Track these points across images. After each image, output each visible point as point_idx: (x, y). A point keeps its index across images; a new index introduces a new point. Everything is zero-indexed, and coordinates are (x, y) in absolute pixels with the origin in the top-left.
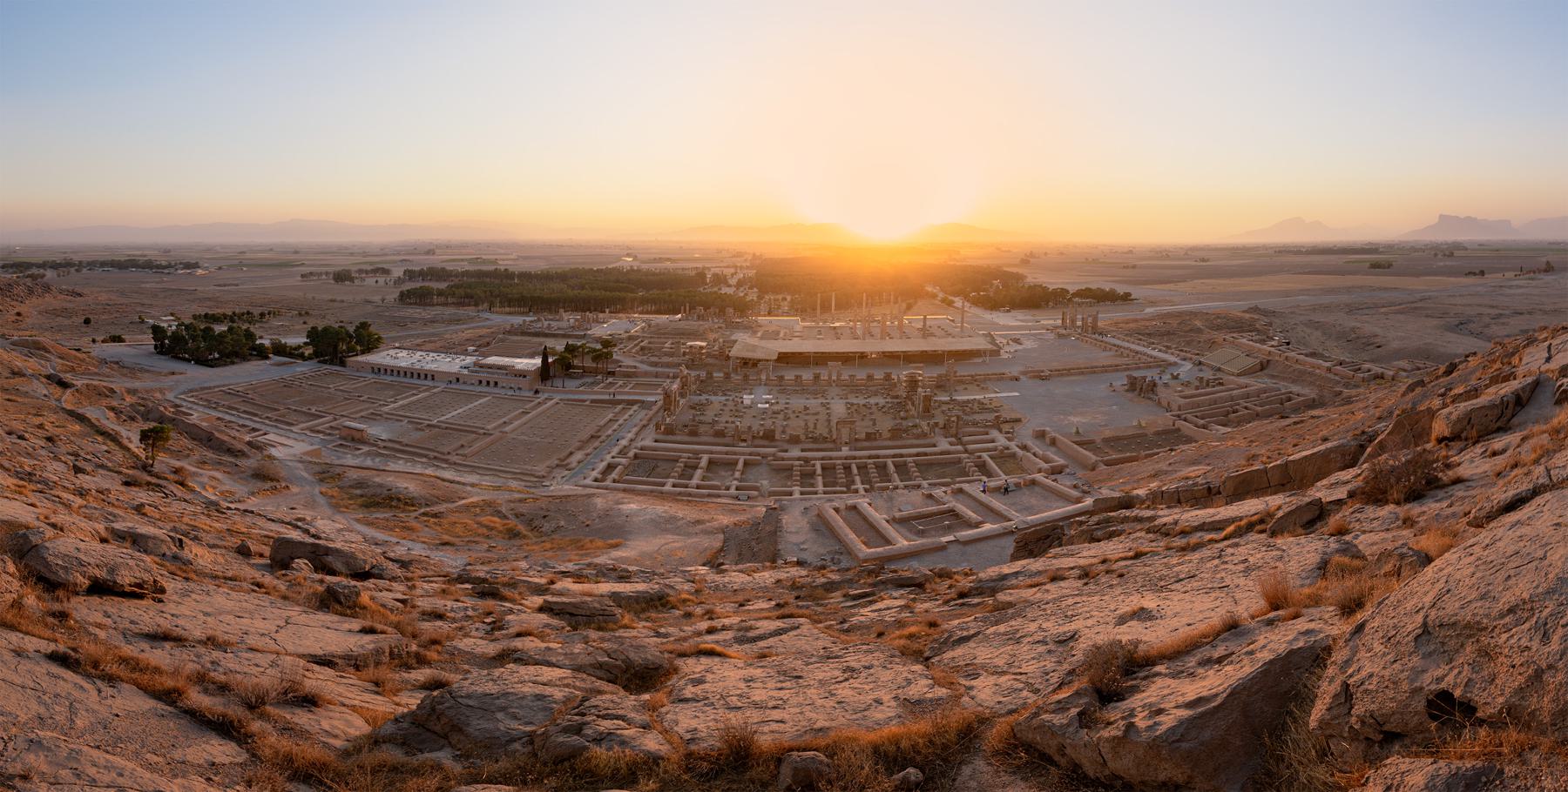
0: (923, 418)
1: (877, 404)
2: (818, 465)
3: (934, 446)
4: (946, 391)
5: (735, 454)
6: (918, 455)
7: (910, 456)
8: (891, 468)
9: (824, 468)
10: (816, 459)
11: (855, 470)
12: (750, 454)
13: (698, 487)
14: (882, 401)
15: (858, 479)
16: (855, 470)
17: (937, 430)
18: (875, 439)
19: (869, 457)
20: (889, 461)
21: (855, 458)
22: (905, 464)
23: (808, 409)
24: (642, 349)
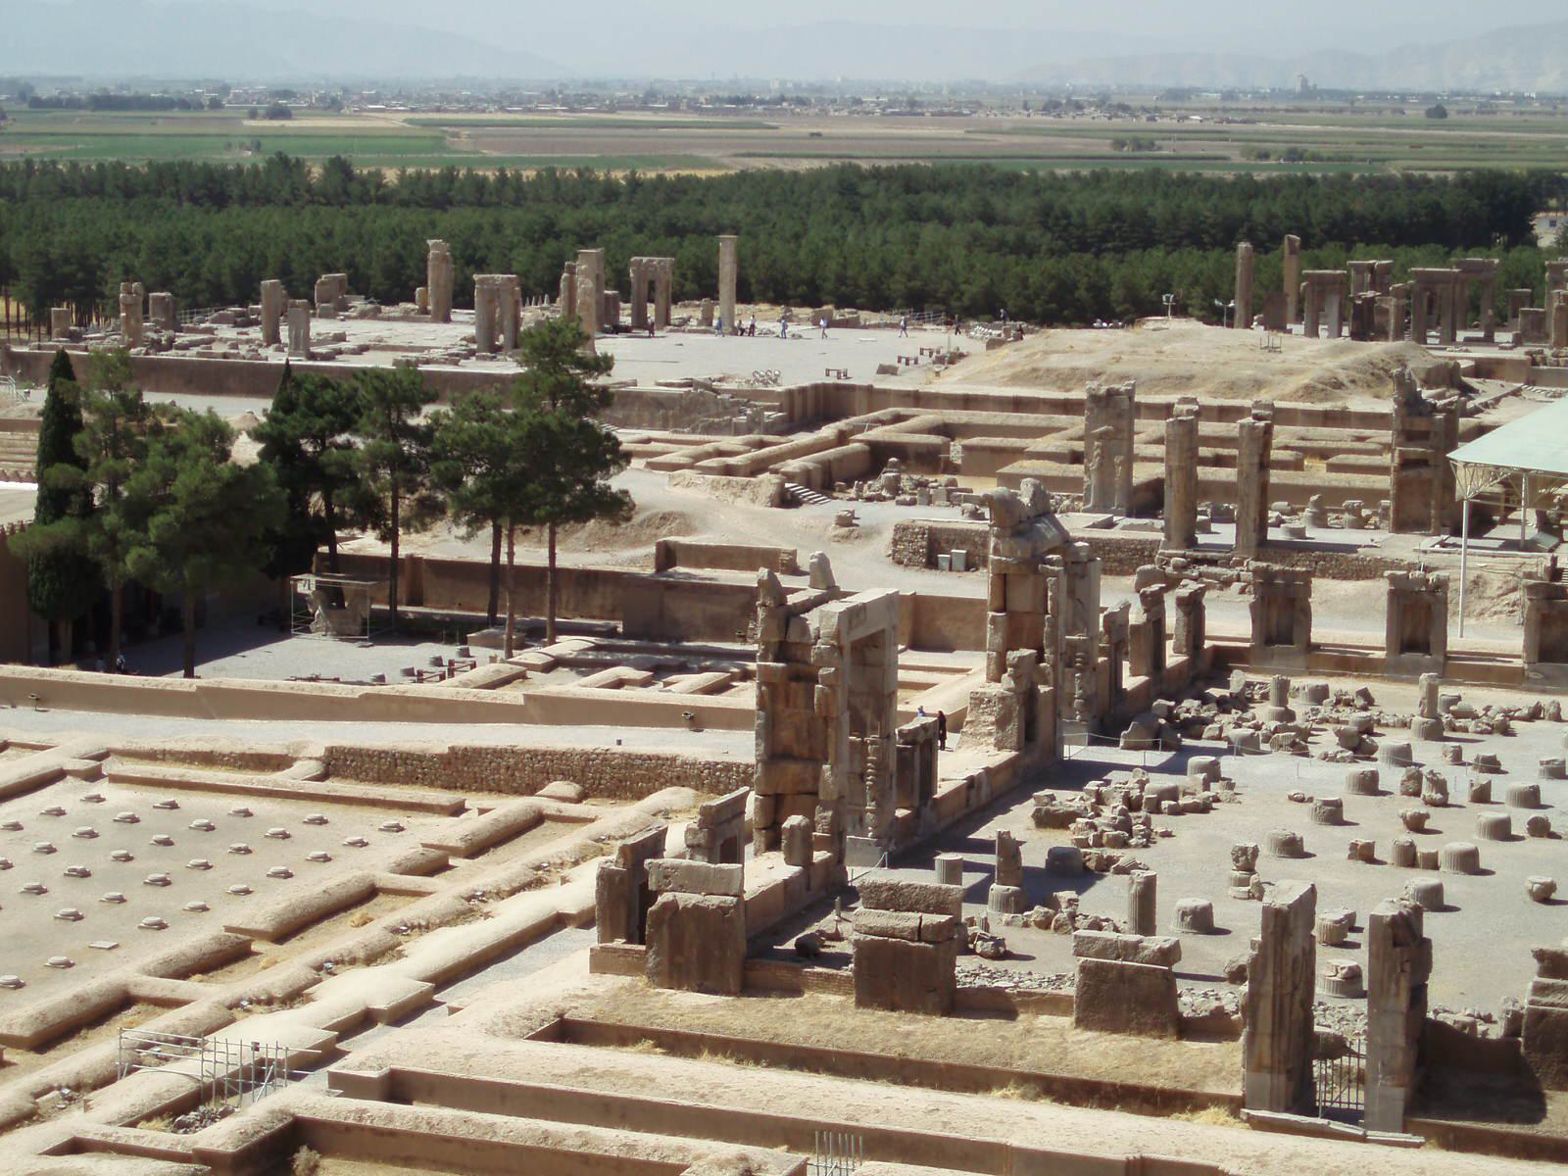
24: (878, 456)
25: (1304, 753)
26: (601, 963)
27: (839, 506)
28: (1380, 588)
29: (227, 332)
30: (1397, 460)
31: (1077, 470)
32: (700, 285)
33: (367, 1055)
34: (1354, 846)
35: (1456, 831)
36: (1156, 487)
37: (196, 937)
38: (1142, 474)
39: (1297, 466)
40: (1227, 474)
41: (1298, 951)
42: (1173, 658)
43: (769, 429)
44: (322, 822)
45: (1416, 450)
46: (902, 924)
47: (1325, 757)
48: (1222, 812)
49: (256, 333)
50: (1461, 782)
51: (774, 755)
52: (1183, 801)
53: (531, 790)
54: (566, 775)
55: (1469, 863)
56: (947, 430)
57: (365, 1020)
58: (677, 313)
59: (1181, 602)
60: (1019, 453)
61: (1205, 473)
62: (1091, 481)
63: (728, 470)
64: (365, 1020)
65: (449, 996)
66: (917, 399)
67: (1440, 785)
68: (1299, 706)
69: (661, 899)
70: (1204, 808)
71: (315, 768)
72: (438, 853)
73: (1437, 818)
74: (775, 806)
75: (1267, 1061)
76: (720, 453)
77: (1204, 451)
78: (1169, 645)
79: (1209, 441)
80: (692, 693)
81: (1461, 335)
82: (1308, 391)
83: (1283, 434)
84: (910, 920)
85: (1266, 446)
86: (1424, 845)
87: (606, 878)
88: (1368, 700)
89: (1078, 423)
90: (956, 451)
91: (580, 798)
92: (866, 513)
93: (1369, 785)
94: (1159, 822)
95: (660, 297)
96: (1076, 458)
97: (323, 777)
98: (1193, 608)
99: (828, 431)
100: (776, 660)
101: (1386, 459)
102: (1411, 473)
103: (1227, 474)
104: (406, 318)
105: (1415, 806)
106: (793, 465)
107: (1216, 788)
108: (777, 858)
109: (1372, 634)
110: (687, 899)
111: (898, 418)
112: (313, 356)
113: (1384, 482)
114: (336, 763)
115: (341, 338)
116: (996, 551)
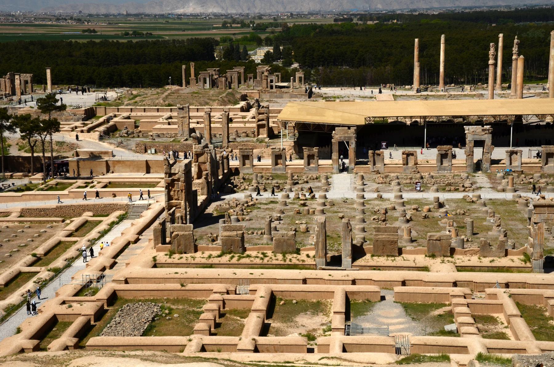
23: (441, 205)
30: (257, 120)
45: (261, 117)
46: (233, 234)
52: (250, 204)
54: (88, 211)
62: (181, 128)
72: (71, 232)
75: (321, 256)
80: (77, 188)
84: (235, 233)
100: (169, 177)
102: (260, 123)
109: (267, 162)
110: (181, 233)
113: (254, 125)
116: (195, 148)
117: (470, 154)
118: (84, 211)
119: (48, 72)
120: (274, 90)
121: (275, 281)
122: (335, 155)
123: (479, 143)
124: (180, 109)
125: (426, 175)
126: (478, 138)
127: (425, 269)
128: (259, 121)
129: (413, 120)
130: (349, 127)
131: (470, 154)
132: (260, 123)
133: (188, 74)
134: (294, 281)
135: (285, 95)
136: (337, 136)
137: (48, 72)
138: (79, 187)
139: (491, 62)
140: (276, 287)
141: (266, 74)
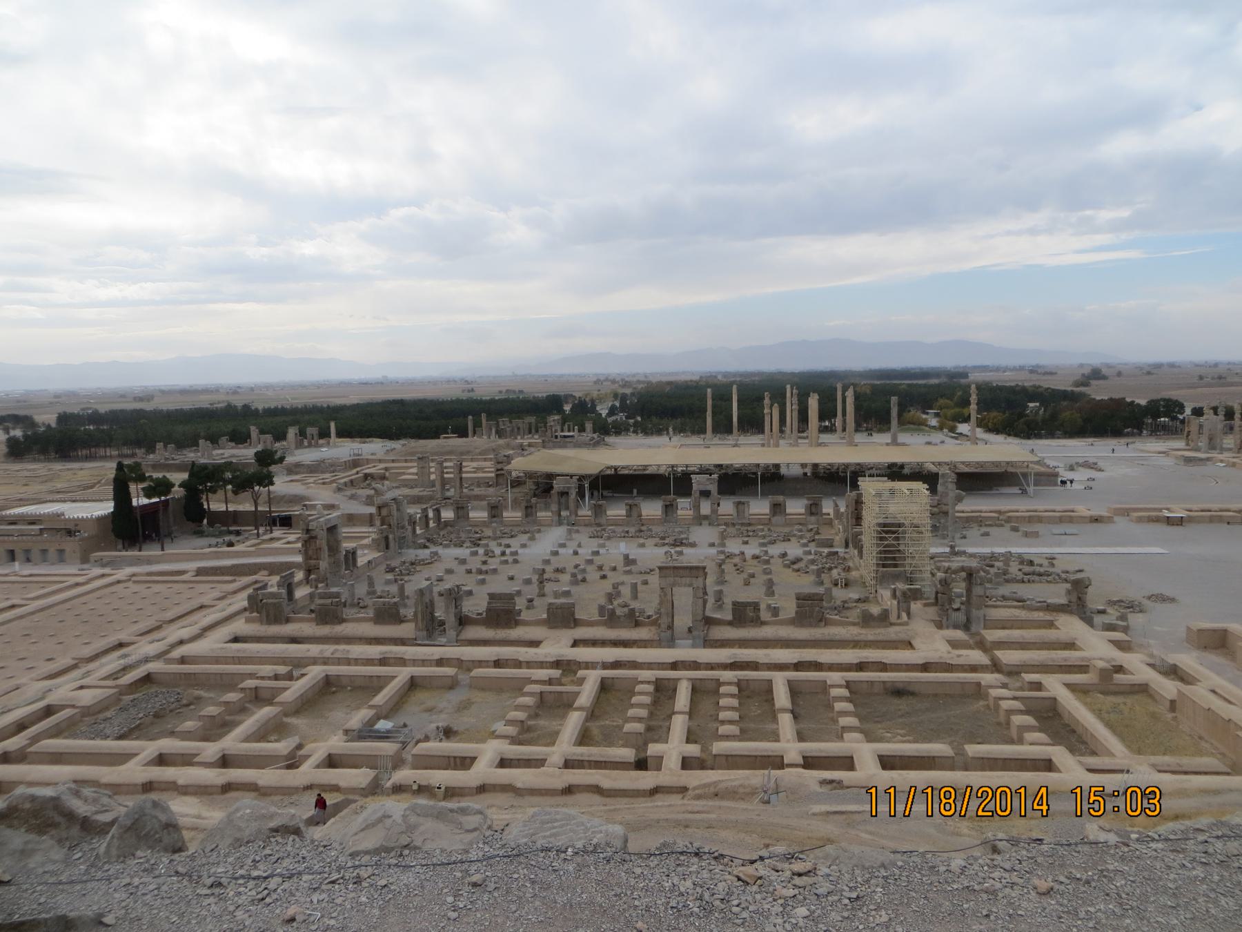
0: (882, 580)
1: (784, 555)
2: (592, 678)
3: (909, 645)
4: (944, 537)
5: (402, 662)
6: (860, 667)
7: (832, 667)
8: (782, 697)
9: (605, 687)
10: (589, 665)
11: (683, 698)
12: (440, 662)
13: (225, 761)
14: (794, 550)
15: (679, 724)
16: (683, 698)
17: (916, 606)
18: (758, 622)
19: (734, 666)
20: (780, 681)
21: (695, 666)
22: (824, 687)
23: (634, 562)
24: (366, 476)
25: (462, 546)
26: (248, 621)
27: (354, 491)
28: (485, 503)
29: (192, 455)
31: (416, 477)
32: (324, 434)
33: (177, 653)
34: (466, 570)
35: (493, 563)
36: (434, 481)
37: (143, 625)
38: (433, 477)
39: (475, 472)
40: (452, 476)
41: (427, 600)
42: (432, 524)
43: (339, 471)
44: (149, 588)
45: (499, 466)
47: (467, 547)
48: (436, 564)
49: (199, 454)
50: (498, 551)
51: (307, 557)
53: (255, 573)
54: (264, 569)
55: (495, 571)
56: (386, 469)
57: (181, 642)
58: (321, 442)
59: (434, 510)
60: (404, 474)
61: (446, 476)
63: (324, 483)
64: (181, 642)
65: (207, 633)
66: (380, 461)
67: (493, 552)
68: (463, 535)
69: (265, 601)
70: (429, 563)
71: (194, 574)
73: (490, 560)
74: (309, 571)
76: (323, 479)
77: (445, 471)
78: (431, 522)
79: (446, 468)
81: (526, 437)
82: (480, 454)
83: (469, 466)
84: (329, 601)
85: (461, 469)
86: (484, 568)
87: (250, 598)
88: (482, 532)
89: (416, 464)
90: (387, 474)
91: (269, 575)
92: (360, 492)
93: (476, 553)
94: (418, 568)
95: (315, 438)
96: (417, 474)
97: (196, 576)
98: (437, 511)
99: (354, 471)
101: (493, 470)
102: (499, 472)
103: (452, 476)
104: (245, 448)
105: (484, 559)
106: (343, 481)
107: (436, 557)
108: (308, 587)
110: (270, 601)
111: (374, 466)
112: (214, 460)
113: (493, 475)
114: (200, 572)
115: (223, 454)
117: (697, 507)
118: (260, 569)
119: (332, 425)
120: (559, 439)
121: (348, 662)
122: (554, 507)
123: (706, 494)
124: (419, 458)
125: (644, 528)
126: (702, 488)
127: (535, 644)
128: (498, 470)
129: (723, 471)
130: (571, 476)
131: (697, 507)
132: (499, 472)
133: (477, 425)
134: (369, 662)
135: (568, 445)
136: (558, 485)
137: (332, 425)
138: (288, 543)
139: (766, 411)
140: (333, 670)
141: (552, 424)
